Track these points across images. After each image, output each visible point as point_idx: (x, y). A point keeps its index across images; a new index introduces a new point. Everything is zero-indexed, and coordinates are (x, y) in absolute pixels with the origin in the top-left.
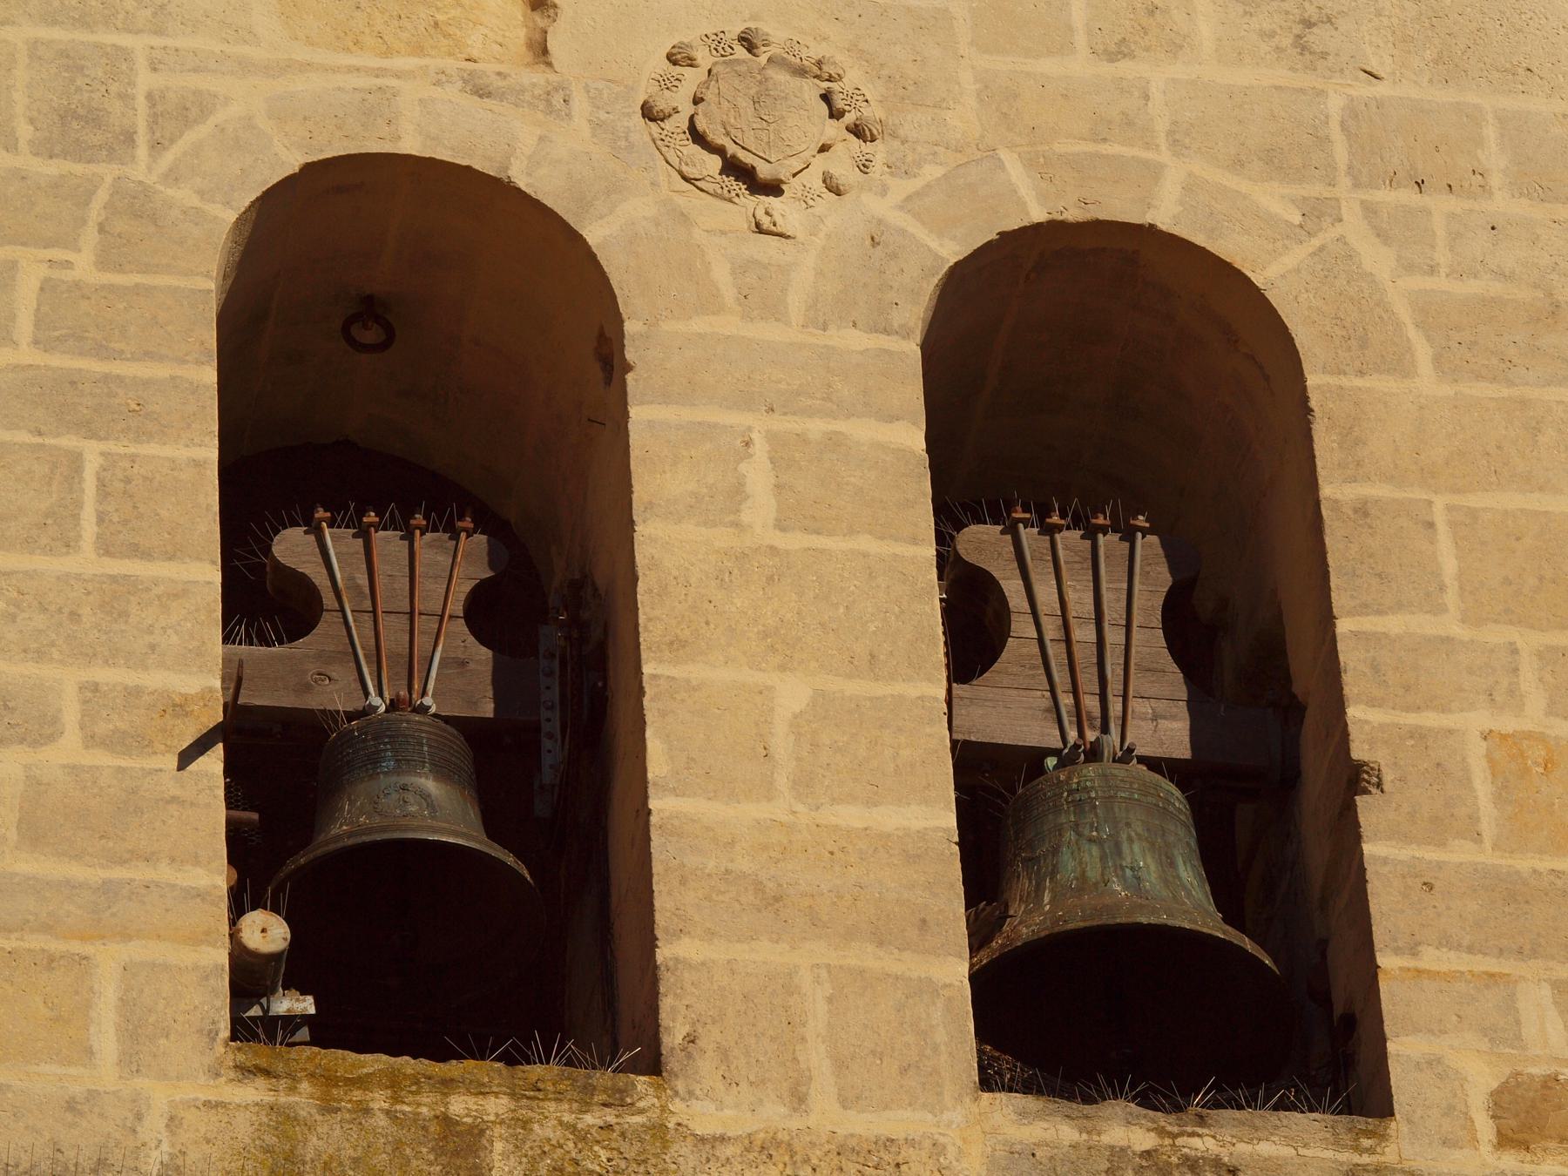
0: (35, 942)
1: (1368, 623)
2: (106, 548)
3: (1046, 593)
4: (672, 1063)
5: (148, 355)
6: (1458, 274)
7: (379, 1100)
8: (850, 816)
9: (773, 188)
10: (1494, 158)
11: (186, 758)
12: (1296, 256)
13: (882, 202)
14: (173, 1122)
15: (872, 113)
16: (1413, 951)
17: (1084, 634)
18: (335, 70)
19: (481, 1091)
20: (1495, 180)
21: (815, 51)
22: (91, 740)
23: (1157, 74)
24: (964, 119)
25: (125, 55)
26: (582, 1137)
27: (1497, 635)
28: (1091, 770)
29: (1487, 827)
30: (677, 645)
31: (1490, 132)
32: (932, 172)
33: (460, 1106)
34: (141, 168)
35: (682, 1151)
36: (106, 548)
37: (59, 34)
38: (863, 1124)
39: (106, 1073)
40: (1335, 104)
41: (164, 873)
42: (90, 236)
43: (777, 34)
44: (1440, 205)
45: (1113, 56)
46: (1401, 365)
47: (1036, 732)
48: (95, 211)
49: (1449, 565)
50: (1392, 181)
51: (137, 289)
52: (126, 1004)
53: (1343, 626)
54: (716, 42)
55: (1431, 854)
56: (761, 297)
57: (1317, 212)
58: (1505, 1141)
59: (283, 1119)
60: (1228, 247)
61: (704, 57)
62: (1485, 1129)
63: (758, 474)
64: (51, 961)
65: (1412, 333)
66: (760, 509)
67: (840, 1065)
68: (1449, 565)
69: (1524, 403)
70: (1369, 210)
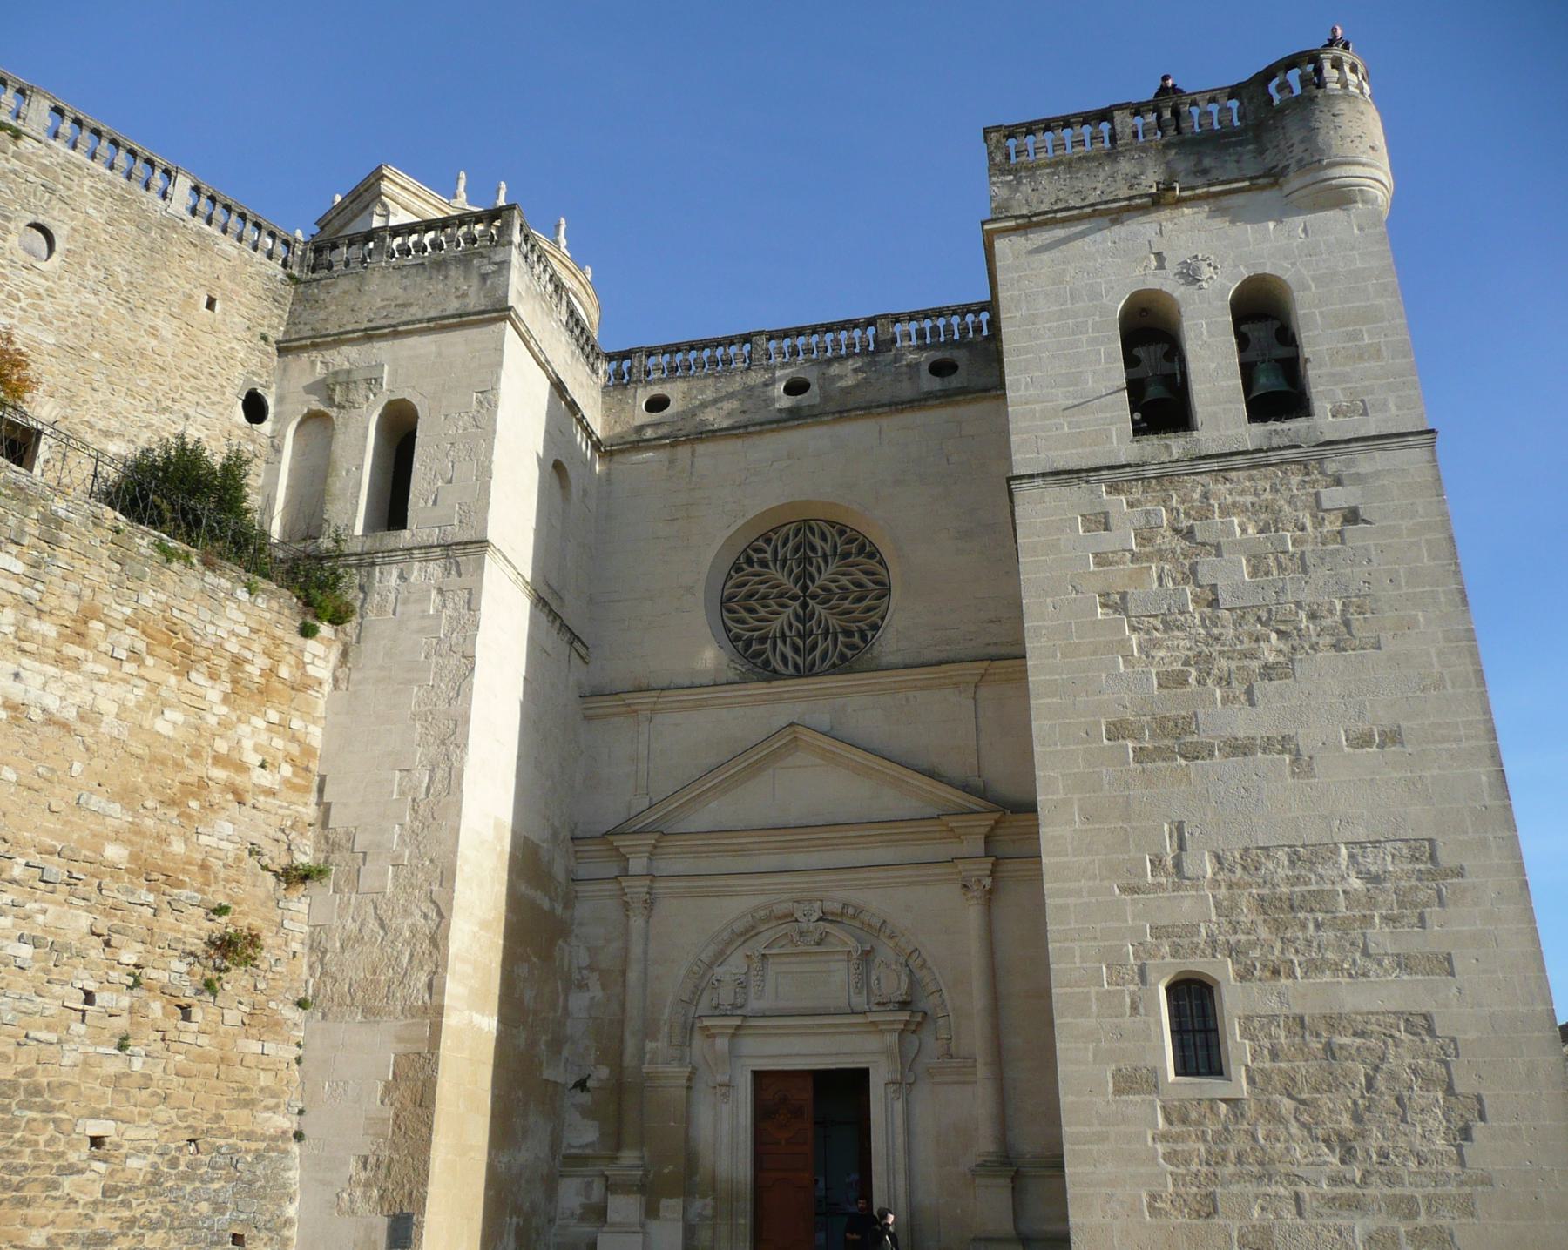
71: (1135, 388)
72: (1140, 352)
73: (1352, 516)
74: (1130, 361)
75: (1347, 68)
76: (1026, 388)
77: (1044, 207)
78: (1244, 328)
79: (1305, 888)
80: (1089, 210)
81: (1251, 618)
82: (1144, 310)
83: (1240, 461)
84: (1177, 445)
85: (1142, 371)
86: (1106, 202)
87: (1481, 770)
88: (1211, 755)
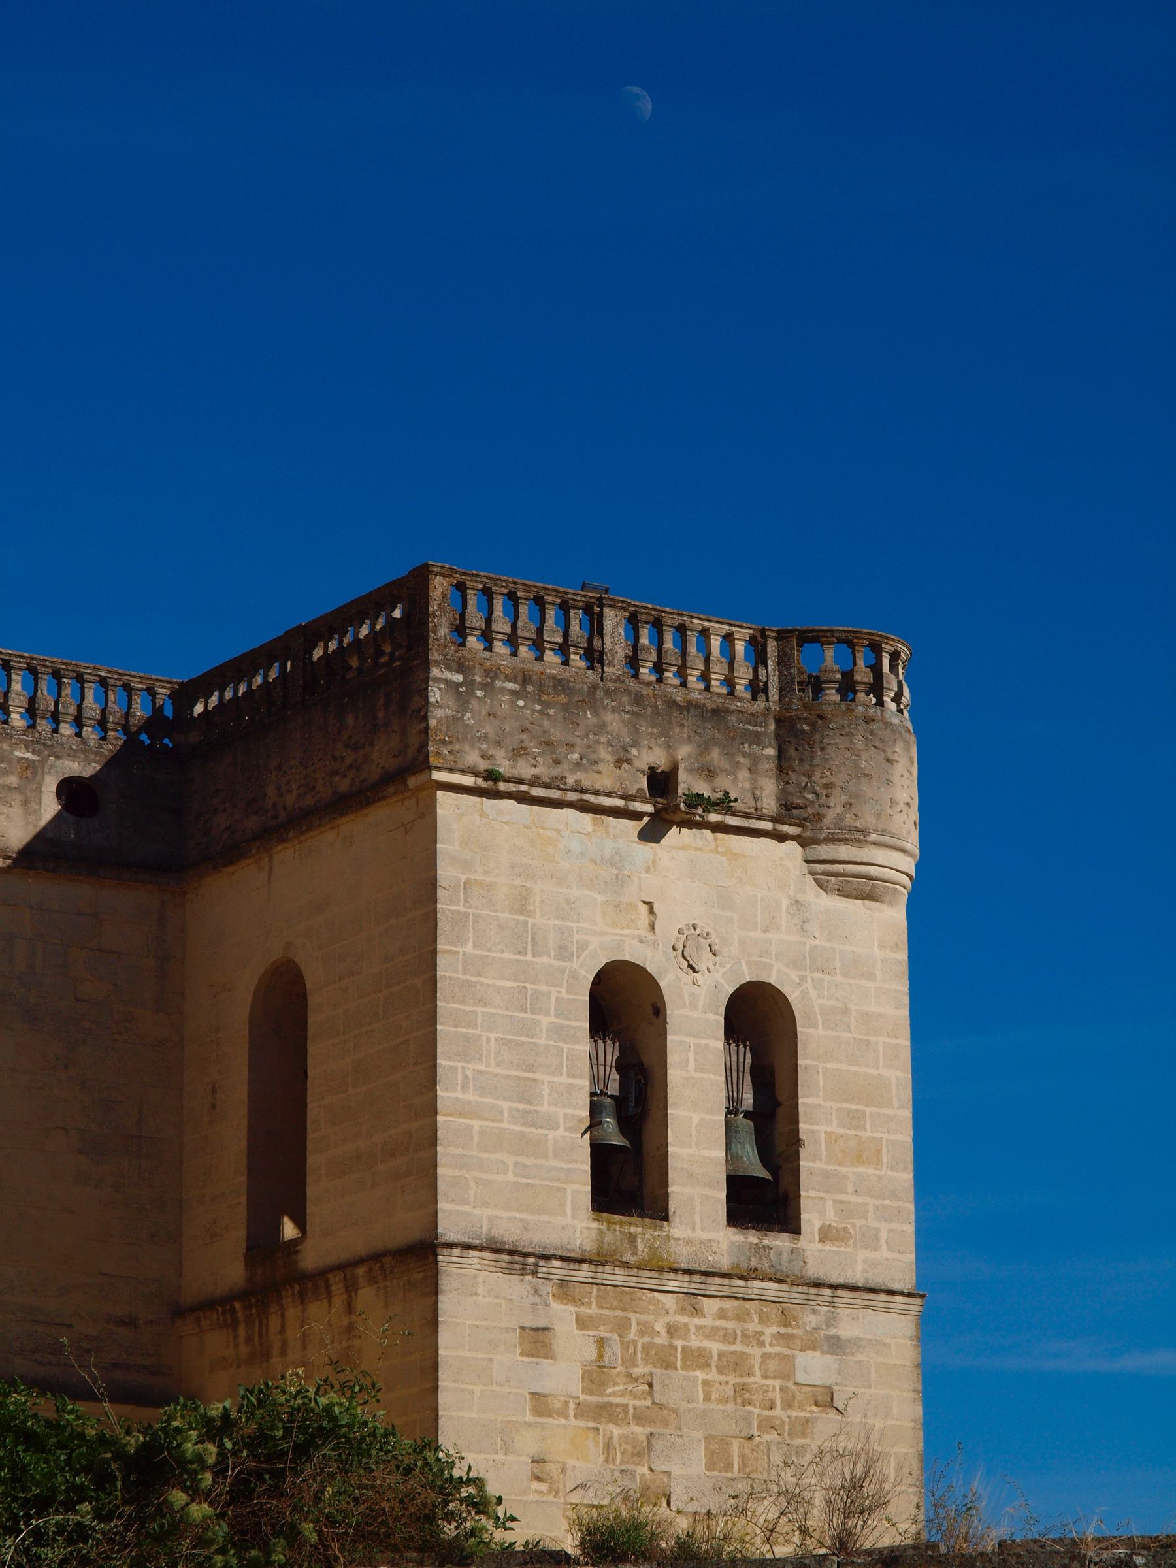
0: (556, 1184)
2: (568, 1076)
5: (576, 1020)
6: (828, 999)
8: (705, 1153)
10: (838, 964)
11: (583, 1135)
12: (797, 993)
13: (718, 976)
16: (807, 1191)
18: (612, 934)
19: (636, 1226)
20: (838, 971)
21: (707, 929)
22: (566, 1129)
24: (734, 949)
25: (571, 929)
27: (830, 1104)
29: (823, 1158)
30: (675, 1104)
31: (837, 956)
32: (728, 966)
33: (633, 1229)
34: (575, 964)
35: (672, 1242)
36: (568, 1076)
38: (705, 1236)
40: (808, 947)
43: (699, 924)
44: (827, 978)
46: (815, 1026)
51: (575, 1000)
53: (800, 1101)
55: (812, 1165)
56: (694, 1006)
57: (803, 979)
58: (820, 1241)
59: (601, 1232)
60: (785, 990)
66: (692, 1066)
67: (702, 1221)
70: (813, 979)
73: (827, 1400)
80: (572, 796)
83: (717, 1285)
84: (640, 1229)
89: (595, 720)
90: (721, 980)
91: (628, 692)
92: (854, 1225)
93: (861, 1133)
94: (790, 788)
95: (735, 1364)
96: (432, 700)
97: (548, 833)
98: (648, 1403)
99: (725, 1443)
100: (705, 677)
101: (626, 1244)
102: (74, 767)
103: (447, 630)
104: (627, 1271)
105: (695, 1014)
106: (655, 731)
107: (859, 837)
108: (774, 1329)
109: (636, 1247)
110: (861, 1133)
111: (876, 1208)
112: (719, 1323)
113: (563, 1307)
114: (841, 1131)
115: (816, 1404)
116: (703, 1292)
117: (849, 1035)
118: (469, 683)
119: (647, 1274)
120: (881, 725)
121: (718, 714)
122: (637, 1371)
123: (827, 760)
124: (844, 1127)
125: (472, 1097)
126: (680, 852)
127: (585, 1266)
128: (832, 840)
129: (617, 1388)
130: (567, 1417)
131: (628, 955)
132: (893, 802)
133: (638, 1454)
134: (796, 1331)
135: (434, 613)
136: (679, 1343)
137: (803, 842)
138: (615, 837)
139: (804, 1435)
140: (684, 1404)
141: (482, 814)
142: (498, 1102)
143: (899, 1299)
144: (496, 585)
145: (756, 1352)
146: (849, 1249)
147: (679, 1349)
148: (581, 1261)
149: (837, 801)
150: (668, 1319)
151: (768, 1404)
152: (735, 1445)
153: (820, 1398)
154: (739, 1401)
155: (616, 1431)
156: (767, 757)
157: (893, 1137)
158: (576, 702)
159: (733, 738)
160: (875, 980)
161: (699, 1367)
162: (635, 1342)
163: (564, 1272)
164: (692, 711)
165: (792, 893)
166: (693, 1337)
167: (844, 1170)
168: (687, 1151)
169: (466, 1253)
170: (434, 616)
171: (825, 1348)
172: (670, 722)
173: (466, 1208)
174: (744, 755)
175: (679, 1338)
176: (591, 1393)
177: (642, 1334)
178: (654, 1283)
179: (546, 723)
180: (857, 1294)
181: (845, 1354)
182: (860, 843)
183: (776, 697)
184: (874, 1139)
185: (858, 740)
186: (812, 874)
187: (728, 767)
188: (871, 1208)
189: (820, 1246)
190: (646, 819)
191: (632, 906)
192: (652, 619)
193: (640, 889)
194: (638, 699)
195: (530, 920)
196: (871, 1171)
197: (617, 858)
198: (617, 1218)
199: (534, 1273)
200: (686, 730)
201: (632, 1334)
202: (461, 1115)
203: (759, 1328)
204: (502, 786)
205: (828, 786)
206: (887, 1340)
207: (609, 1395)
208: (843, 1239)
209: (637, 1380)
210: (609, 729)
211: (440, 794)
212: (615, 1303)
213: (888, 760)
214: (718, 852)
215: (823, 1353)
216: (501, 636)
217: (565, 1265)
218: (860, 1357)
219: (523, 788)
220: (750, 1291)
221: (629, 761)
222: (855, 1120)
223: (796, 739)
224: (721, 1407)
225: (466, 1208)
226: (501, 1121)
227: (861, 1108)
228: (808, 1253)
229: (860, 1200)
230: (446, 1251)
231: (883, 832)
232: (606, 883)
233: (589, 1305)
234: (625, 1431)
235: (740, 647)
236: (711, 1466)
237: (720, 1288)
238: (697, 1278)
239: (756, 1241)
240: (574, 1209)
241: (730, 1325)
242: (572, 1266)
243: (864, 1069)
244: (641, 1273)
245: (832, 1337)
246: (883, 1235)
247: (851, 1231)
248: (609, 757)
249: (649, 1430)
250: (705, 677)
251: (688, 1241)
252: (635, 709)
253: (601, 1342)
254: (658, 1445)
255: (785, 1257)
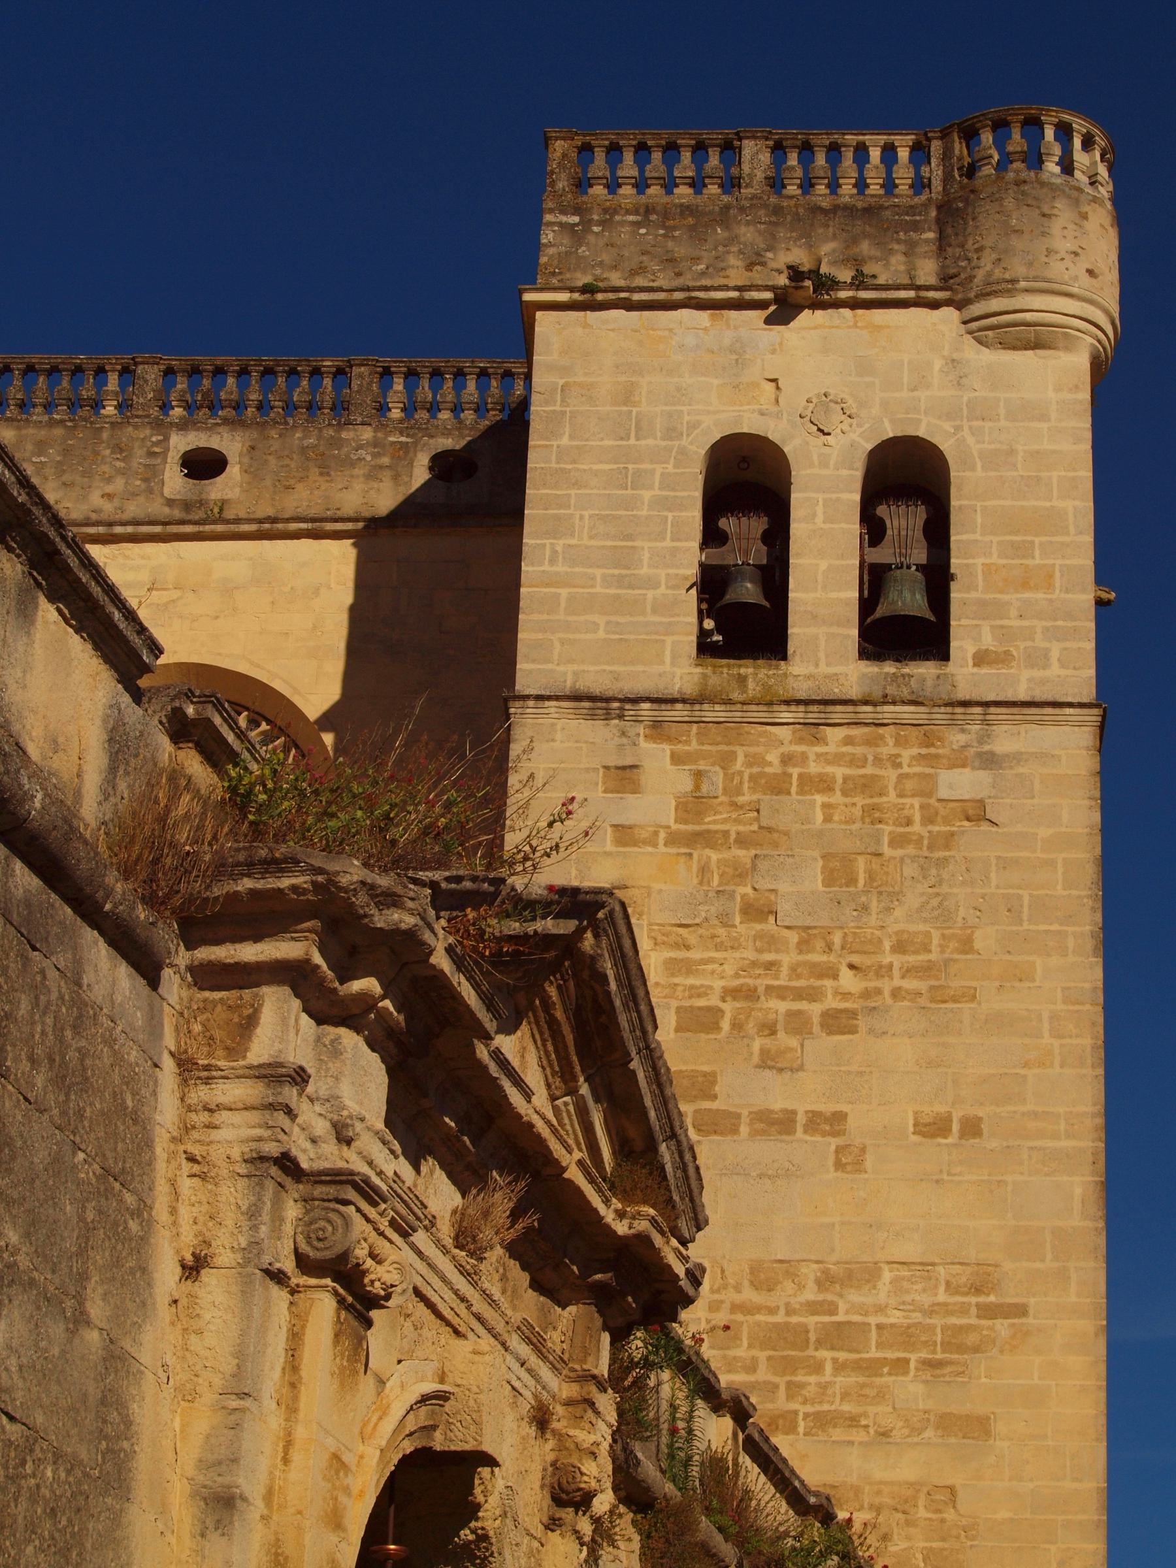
0: (654, 637)
1: (958, 537)
2: (672, 540)
3: (896, 523)
4: (789, 657)
5: (684, 490)
6: (989, 443)
7: (725, 670)
8: (834, 595)
9: (829, 434)
11: (688, 590)
12: (952, 441)
14: (681, 678)
15: (854, 411)
16: (959, 620)
17: (903, 533)
19: (747, 667)
20: (1002, 417)
22: (668, 587)
23: (923, 394)
24: (875, 411)
25: (682, 411)
26: (768, 676)
27: (988, 538)
28: (898, 571)
29: (980, 589)
30: (798, 554)
31: (1002, 404)
32: (867, 426)
33: (743, 671)
34: (684, 442)
35: (791, 680)
36: (672, 540)
37: (668, 408)
38: (831, 670)
39: (667, 667)
40: (965, 399)
41: (682, 619)
42: (672, 461)
43: (832, 391)
44: (988, 424)
45: (912, 391)
46: (973, 468)
47: (889, 560)
48: (674, 454)
49: (979, 520)
50: (977, 419)
51: (683, 473)
52: (672, 650)
54: (818, 396)
56: (824, 464)
57: (958, 428)
58: (975, 665)
59: (705, 676)
60: (935, 440)
61: (814, 400)
62: (971, 662)
63: (820, 510)
64: (657, 641)
65: (977, 460)
67: (827, 656)
68: (979, 520)
69: (1001, 477)
70: (970, 427)
71: (712, 585)
72: (727, 524)
73: (977, 813)
74: (712, 536)
75: (1077, 142)
76: (552, 561)
77: (616, 279)
78: (882, 510)
79: (826, 1319)
81: (819, 944)
82: (744, 459)
83: (838, 713)
84: (755, 674)
85: (728, 556)
86: (706, 289)
87: (1077, 1179)
88: (735, 1130)
89: (726, 234)
90: (857, 439)
91: (765, 206)
92: (1017, 647)
93: (1029, 562)
94: (948, 262)
95: (868, 785)
96: (544, 241)
97: (659, 333)
98: (755, 827)
99: (847, 860)
100: (861, 185)
101: (734, 684)
102: (447, 443)
103: (566, 183)
104: (728, 707)
105: (824, 472)
106: (794, 234)
107: (1009, 287)
108: (915, 751)
109: (746, 686)
110: (1029, 562)
111: (1046, 629)
112: (844, 749)
113: (655, 745)
114: (1004, 561)
115: (968, 819)
116: (823, 721)
117: (1016, 473)
118: (587, 224)
119: (754, 708)
120: (1035, 185)
121: (870, 212)
122: (741, 800)
123: (977, 227)
124: (1007, 557)
125: (560, 568)
126: (812, 332)
127: (679, 706)
128: (984, 295)
129: (718, 817)
130: (655, 845)
131: (747, 426)
132: (1049, 252)
133: (740, 876)
134: (941, 751)
135: (552, 172)
136: (795, 772)
137: (960, 306)
138: (736, 328)
139: (947, 847)
140: (798, 826)
141: (586, 325)
142: (590, 571)
143: (1068, 711)
144: (623, 139)
145: (891, 775)
146: (1012, 671)
147: (795, 777)
148: (673, 701)
149: (987, 259)
150: (782, 749)
151: (904, 821)
152: (861, 863)
153: (971, 812)
154: (867, 820)
155: (714, 856)
156: (927, 241)
157: (1068, 562)
158: (699, 221)
159: (888, 229)
160: (1049, 420)
161: (818, 792)
162: (740, 773)
163: (656, 713)
164: (839, 213)
165: (946, 353)
166: (812, 764)
167: (1006, 597)
168: (812, 595)
169: (540, 704)
170: (552, 172)
171: (977, 764)
172: (812, 225)
173: (550, 666)
174: (899, 242)
175: (794, 766)
176: (686, 822)
177: (750, 765)
178: (763, 716)
179: (670, 244)
180: (1015, 710)
181: (1001, 768)
182: (1010, 293)
183: (940, 188)
184: (1045, 565)
185: (1009, 203)
186: (970, 333)
187: (878, 254)
188: (1039, 630)
189: (975, 670)
190: (772, 308)
191: (756, 385)
192: (799, 143)
193: (763, 369)
194: (777, 211)
195: (635, 410)
196: (1040, 595)
197: (738, 345)
198: (724, 661)
199: (621, 717)
200: (831, 229)
201: (739, 764)
202: (547, 585)
203: (894, 751)
204: (600, 297)
205: (980, 250)
206: (1057, 752)
207: (709, 823)
208: (1003, 662)
209: (741, 807)
210: (742, 239)
211: (539, 314)
212: (719, 739)
213: (1044, 215)
214: (857, 327)
215: (973, 768)
216: (628, 181)
217: (655, 706)
218: (1021, 770)
219: (623, 295)
220: (880, 716)
221: (763, 264)
222: (1023, 550)
223: (952, 217)
224: (843, 827)
225: (550, 666)
226: (593, 586)
227: (1029, 538)
228: (959, 678)
229: (1026, 623)
230: (518, 704)
231: (1035, 279)
232: (724, 368)
233: (688, 742)
234: (726, 855)
235: (903, 154)
236: (829, 881)
237: (843, 716)
238: (815, 708)
239: (892, 670)
240: (674, 657)
241: (859, 750)
242: (663, 707)
243: (1033, 503)
244: (745, 708)
245: (986, 753)
246: (1055, 654)
247: (1015, 653)
248: (740, 263)
249: (753, 852)
250: (861, 185)
251: (808, 677)
252: (773, 219)
253: (698, 775)
254: (762, 865)
255: (929, 683)
